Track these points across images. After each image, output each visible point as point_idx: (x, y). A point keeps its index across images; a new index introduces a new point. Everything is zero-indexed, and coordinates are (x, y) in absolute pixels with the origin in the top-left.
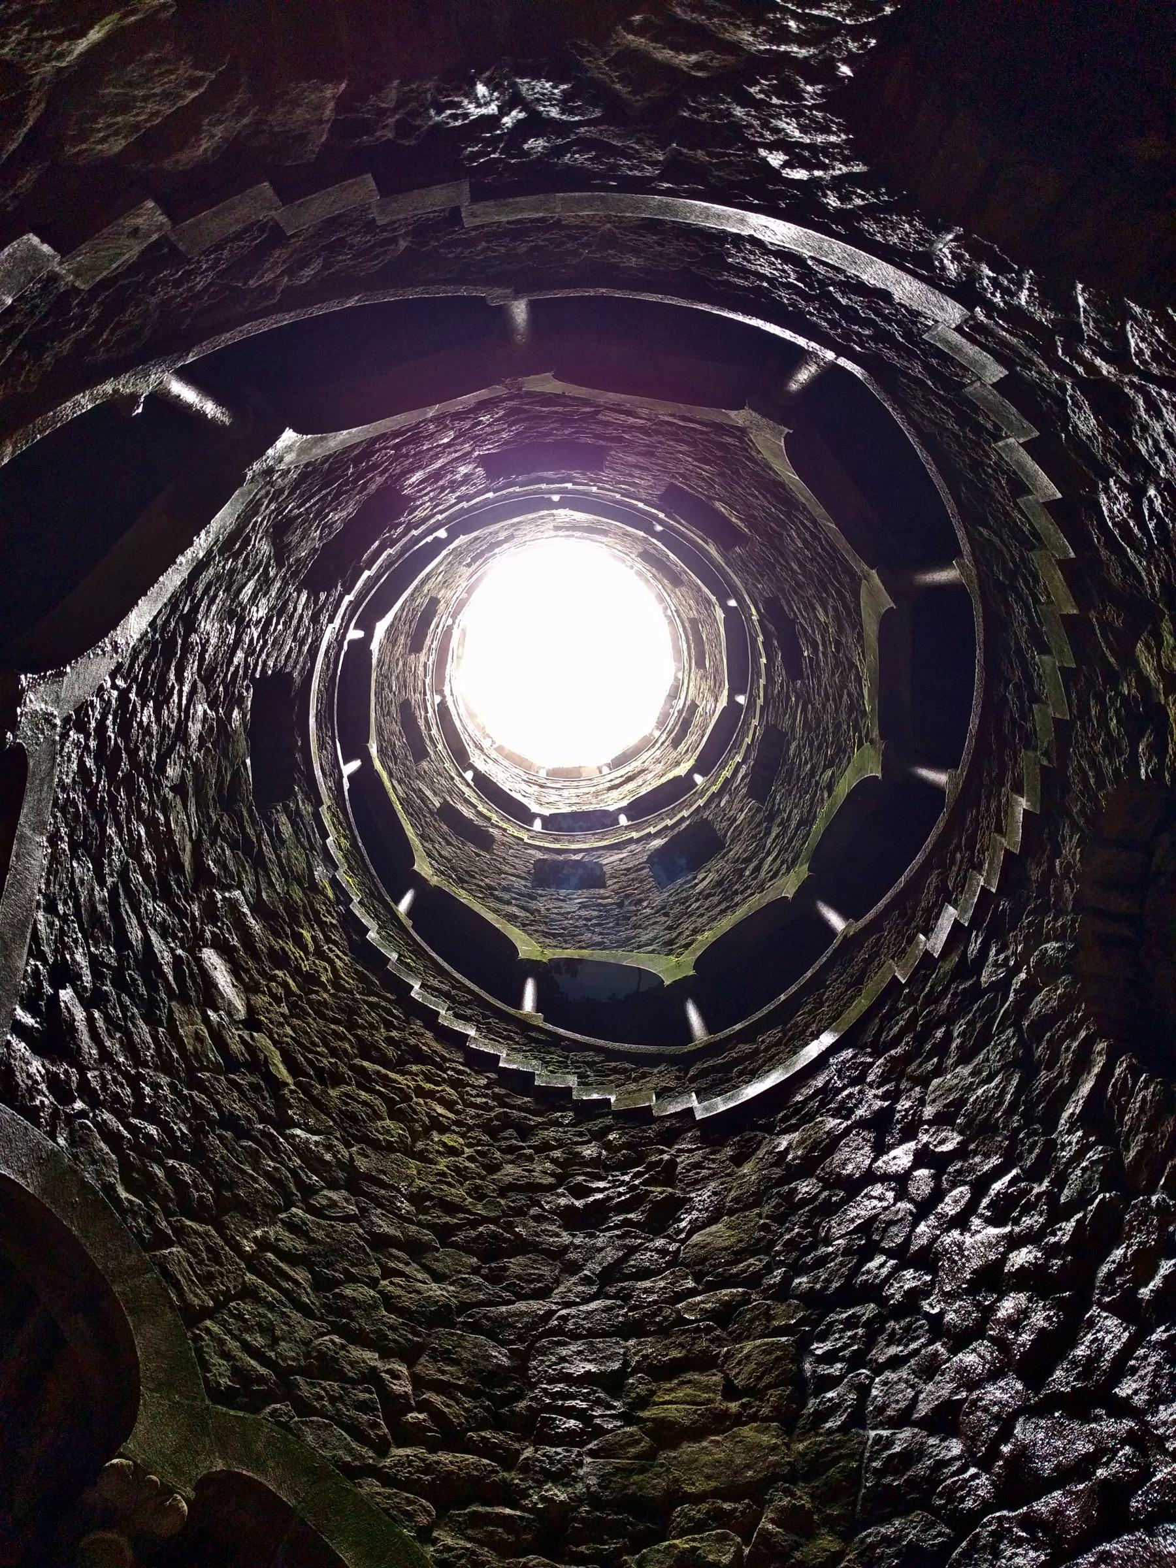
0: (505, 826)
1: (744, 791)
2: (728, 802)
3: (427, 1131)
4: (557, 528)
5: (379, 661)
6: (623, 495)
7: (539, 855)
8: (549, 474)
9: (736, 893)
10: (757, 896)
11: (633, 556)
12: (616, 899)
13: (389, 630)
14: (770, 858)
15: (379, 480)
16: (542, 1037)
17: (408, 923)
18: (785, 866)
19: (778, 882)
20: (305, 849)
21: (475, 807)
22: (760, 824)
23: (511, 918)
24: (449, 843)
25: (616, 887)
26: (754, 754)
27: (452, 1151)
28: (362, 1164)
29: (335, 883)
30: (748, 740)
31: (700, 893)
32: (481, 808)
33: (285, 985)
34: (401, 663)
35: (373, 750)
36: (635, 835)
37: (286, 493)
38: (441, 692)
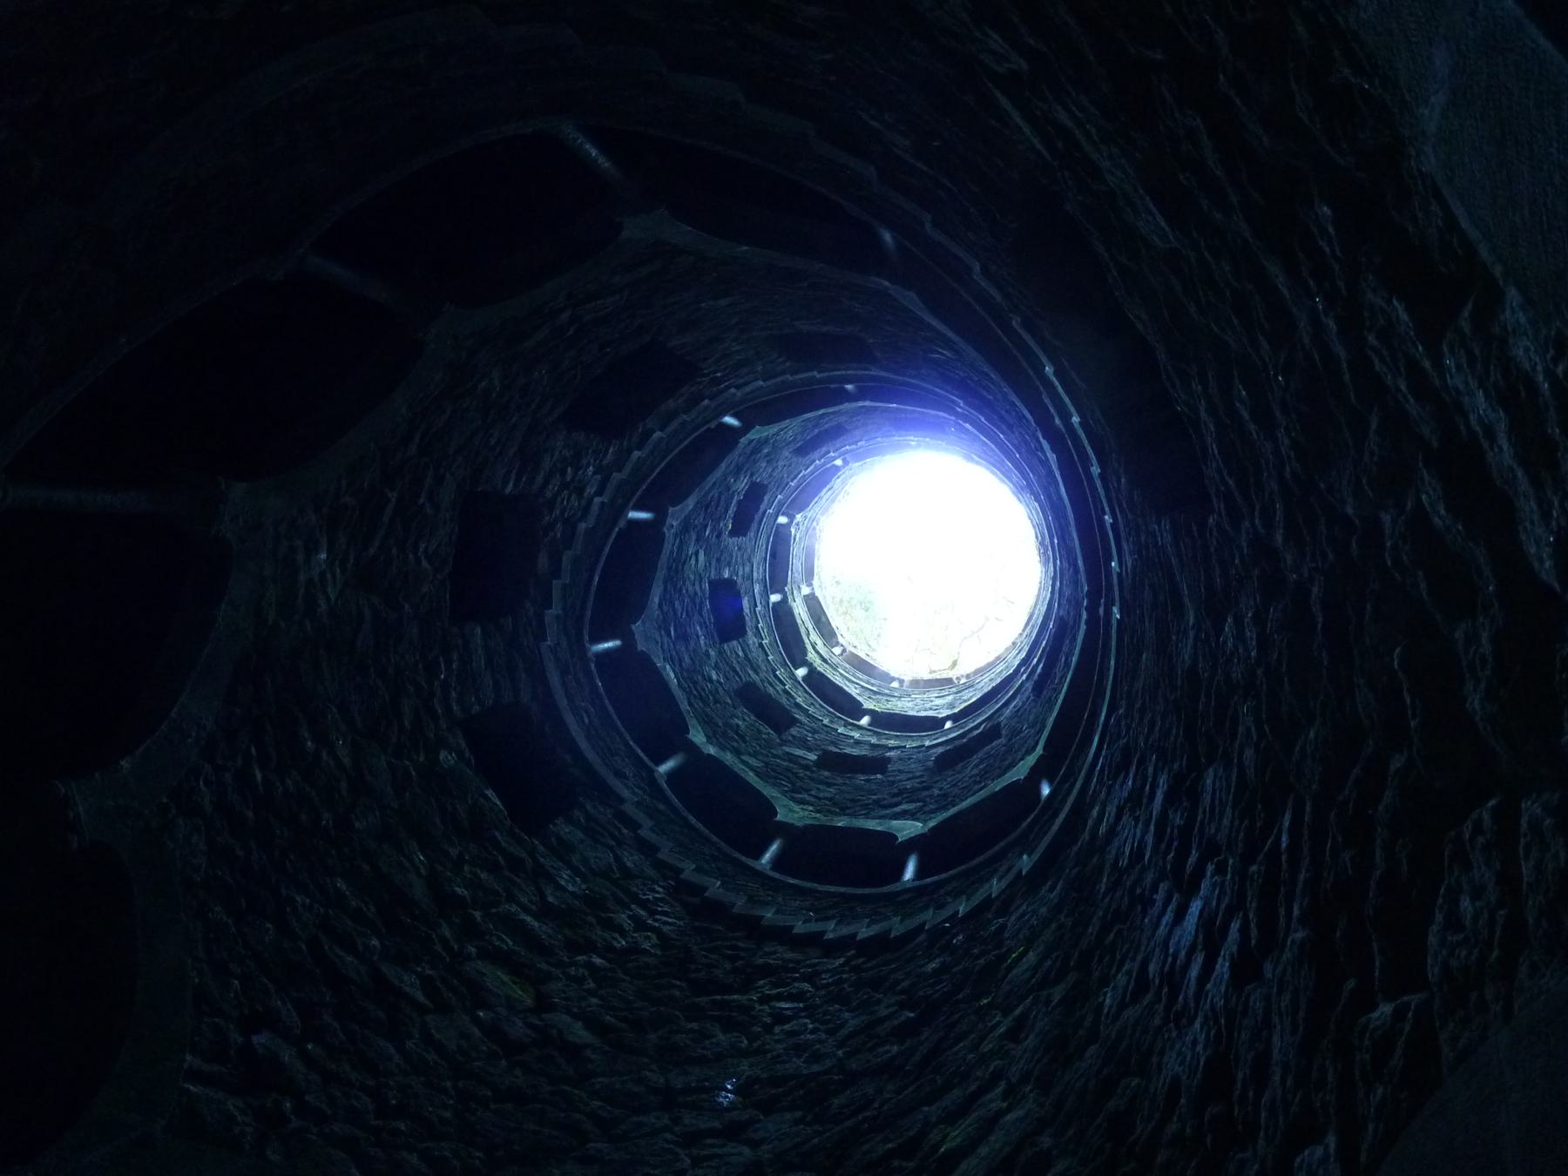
3: (768, 1029)
7: (940, 750)
8: (671, 404)
16: (907, 896)
20: (611, 848)
23: (896, 816)
24: (829, 785)
27: (793, 1033)
28: (678, 1083)
29: (660, 865)
33: (589, 965)
38: (805, 663)
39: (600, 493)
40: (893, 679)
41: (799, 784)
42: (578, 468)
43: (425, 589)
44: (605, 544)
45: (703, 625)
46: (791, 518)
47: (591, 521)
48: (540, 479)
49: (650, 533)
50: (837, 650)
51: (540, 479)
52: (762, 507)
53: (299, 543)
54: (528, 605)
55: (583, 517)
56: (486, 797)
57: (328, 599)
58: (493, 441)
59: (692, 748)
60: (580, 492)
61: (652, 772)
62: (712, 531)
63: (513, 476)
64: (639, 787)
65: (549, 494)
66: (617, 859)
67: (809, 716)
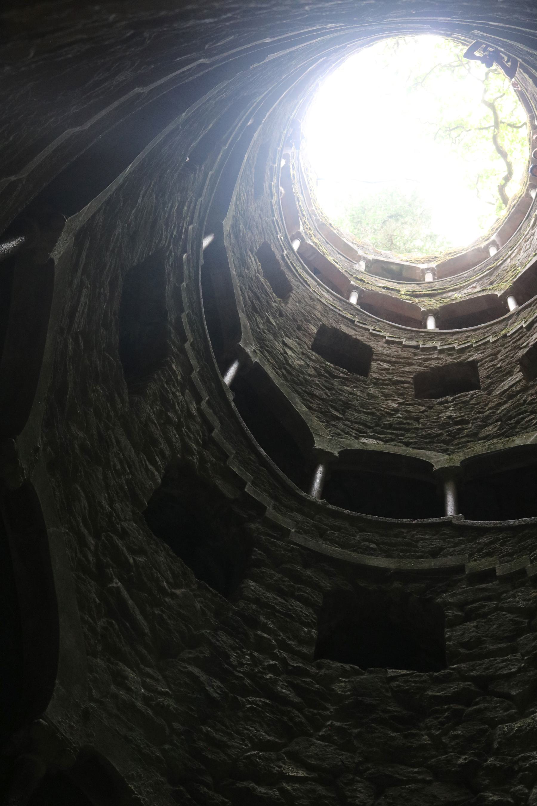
13: (328, 419)
20: (497, 609)
34: (372, 390)
37: (122, 666)
38: (426, 315)
39: (199, 401)
40: (487, 248)
42: (173, 407)
43: (198, 606)
44: (239, 423)
45: (345, 381)
46: (298, 236)
47: (217, 424)
48: (163, 445)
49: (250, 374)
50: (429, 278)
51: (163, 445)
52: (278, 257)
53: (113, 688)
54: (252, 526)
56: (393, 679)
57: (166, 694)
58: (119, 467)
59: (447, 473)
60: (190, 415)
61: (449, 524)
62: (274, 318)
63: (150, 467)
64: (456, 545)
66: (510, 610)
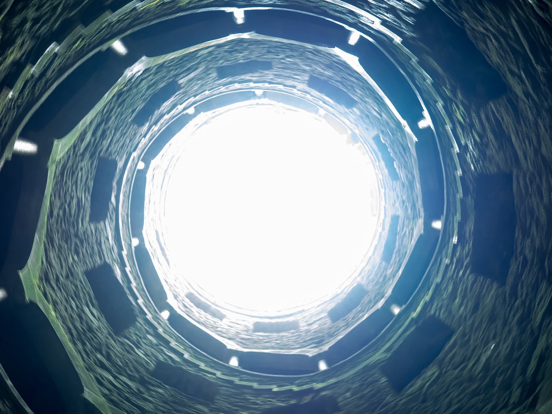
0: (148, 136)
1: (161, 358)
2: (151, 342)
4: (395, 219)
5: (319, 52)
6: (438, 286)
7: (120, 164)
8: (470, 226)
9: (84, 344)
10: (82, 363)
11: (359, 279)
12: (81, 231)
14: (111, 378)
15: (518, 90)
17: (104, 47)
18: (107, 392)
19: (95, 385)
21: (168, 112)
22: (138, 371)
25: (89, 232)
26: (191, 370)
30: (202, 366)
31: (83, 311)
32: (167, 117)
34: (307, 68)
35: (246, 36)
36: (125, 253)
41: (165, 70)
45: (330, 78)
55: (445, 107)
65: (474, 115)
67: (220, 85)
